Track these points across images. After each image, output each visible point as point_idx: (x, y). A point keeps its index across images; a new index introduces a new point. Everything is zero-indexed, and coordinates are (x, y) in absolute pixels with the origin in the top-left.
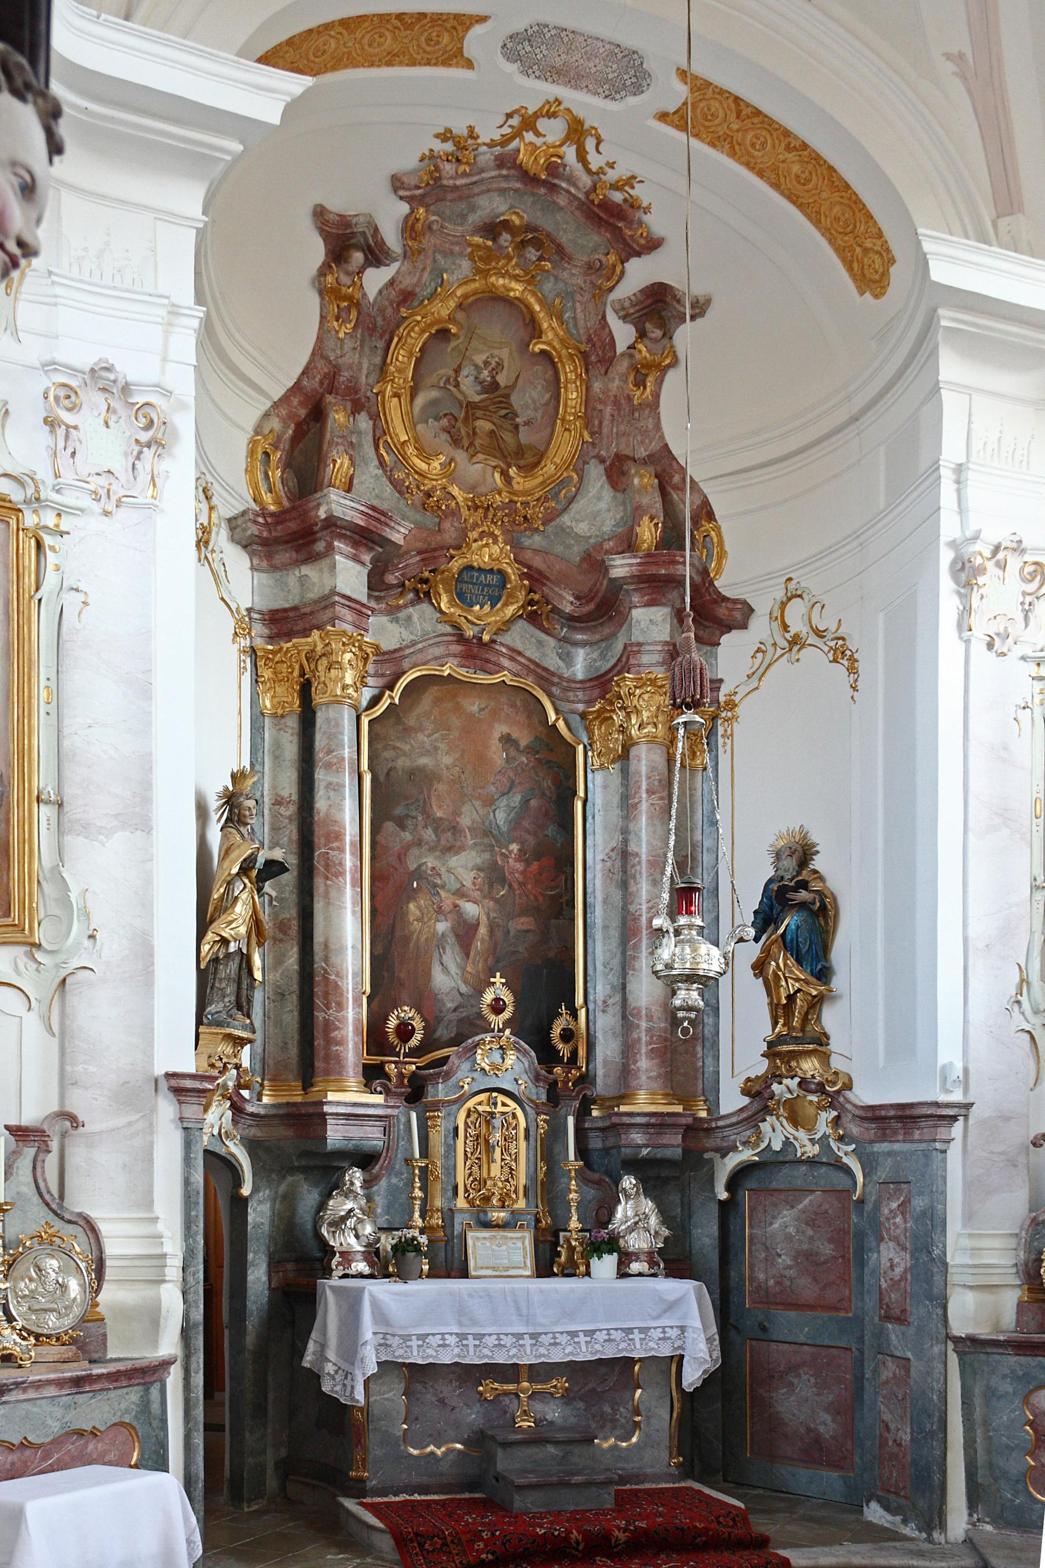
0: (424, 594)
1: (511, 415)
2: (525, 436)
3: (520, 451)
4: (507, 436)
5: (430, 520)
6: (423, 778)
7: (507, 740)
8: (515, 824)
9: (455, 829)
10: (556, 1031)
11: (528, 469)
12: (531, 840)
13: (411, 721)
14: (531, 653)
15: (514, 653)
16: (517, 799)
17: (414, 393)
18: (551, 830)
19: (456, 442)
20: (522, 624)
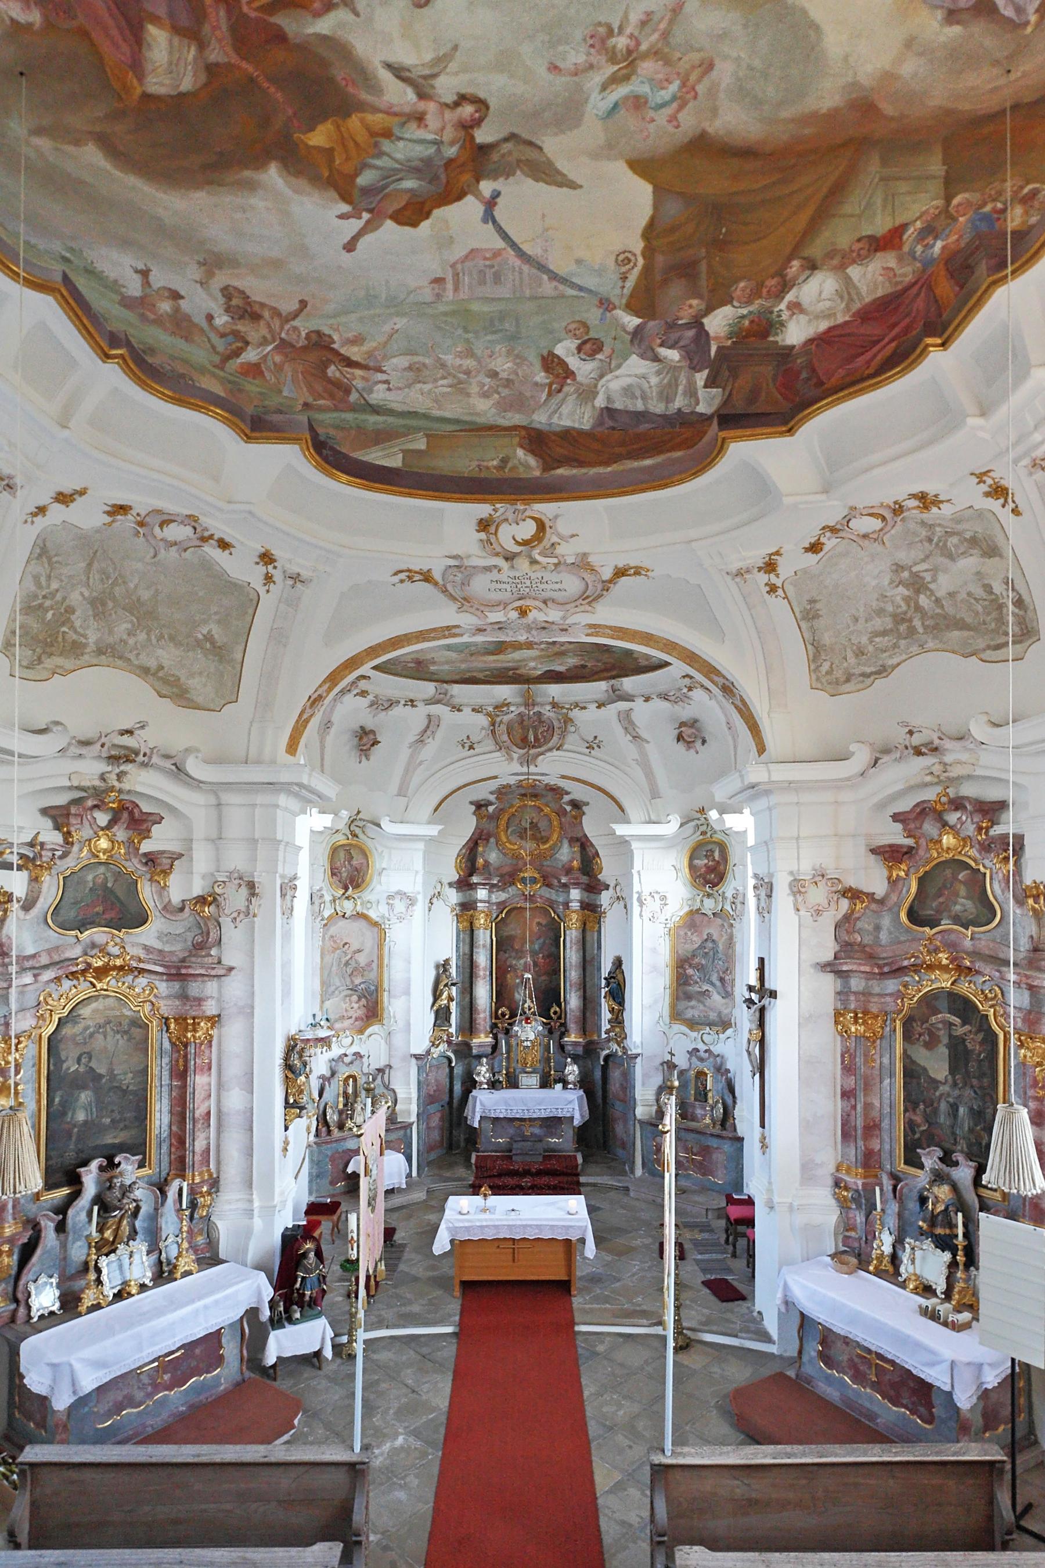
0: (513, 884)
1: (539, 829)
2: (543, 834)
3: (542, 838)
4: (538, 835)
5: (514, 862)
6: (511, 938)
7: (539, 924)
8: (541, 948)
9: (522, 952)
10: (552, 1011)
11: (544, 843)
12: (546, 953)
13: (508, 921)
14: (548, 896)
15: (541, 897)
16: (541, 940)
17: (508, 827)
18: (553, 949)
19: (522, 838)
20: (544, 888)
